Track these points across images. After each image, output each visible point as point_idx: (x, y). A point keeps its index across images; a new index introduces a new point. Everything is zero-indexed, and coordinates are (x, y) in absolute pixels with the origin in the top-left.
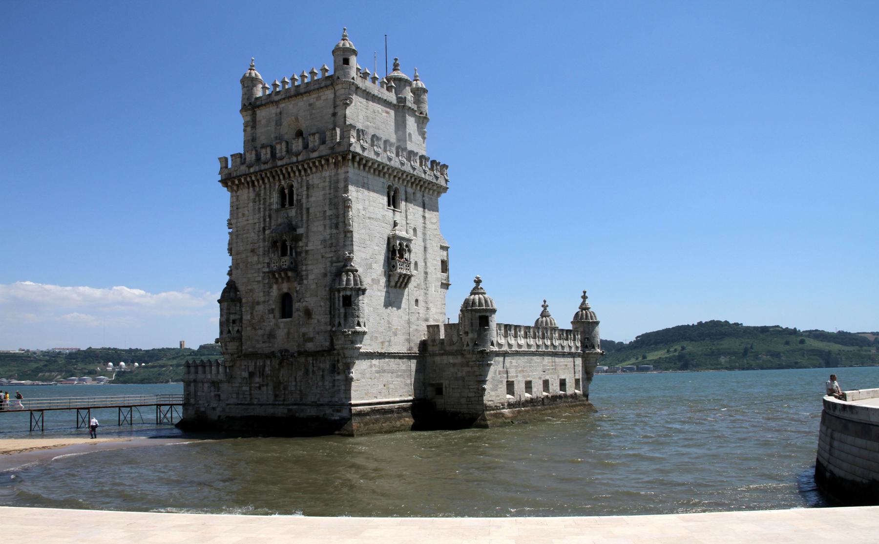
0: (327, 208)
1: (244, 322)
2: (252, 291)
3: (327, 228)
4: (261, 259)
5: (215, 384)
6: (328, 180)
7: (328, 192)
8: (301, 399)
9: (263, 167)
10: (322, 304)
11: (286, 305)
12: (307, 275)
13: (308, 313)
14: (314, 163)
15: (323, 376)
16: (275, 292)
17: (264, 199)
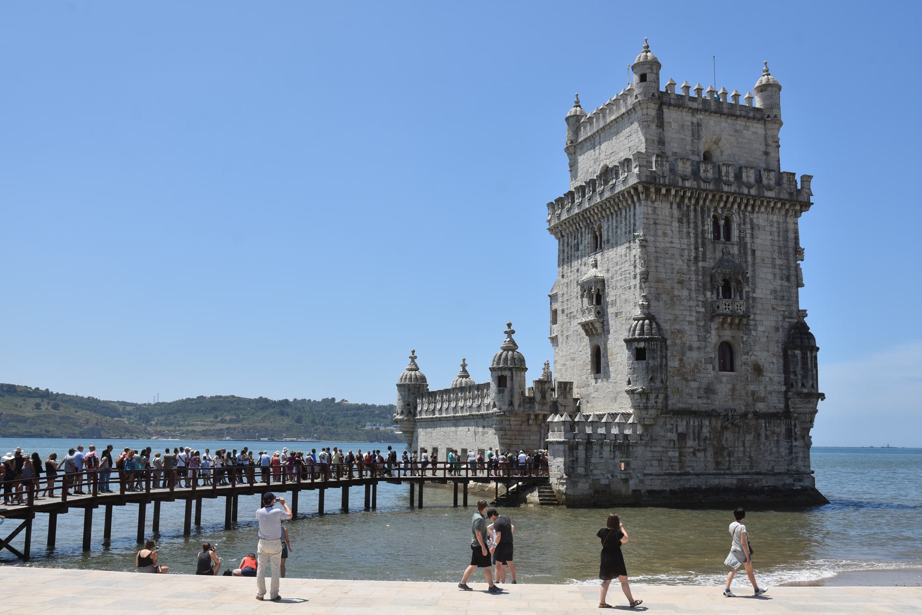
0: (776, 255)
1: (669, 369)
2: (679, 331)
3: (778, 278)
4: (694, 295)
5: (623, 446)
6: (775, 225)
7: (776, 238)
8: (751, 467)
9: (703, 185)
10: (775, 361)
11: (727, 356)
12: (755, 325)
13: (758, 370)
14: (768, 202)
15: (778, 441)
16: (713, 338)
17: (695, 223)
